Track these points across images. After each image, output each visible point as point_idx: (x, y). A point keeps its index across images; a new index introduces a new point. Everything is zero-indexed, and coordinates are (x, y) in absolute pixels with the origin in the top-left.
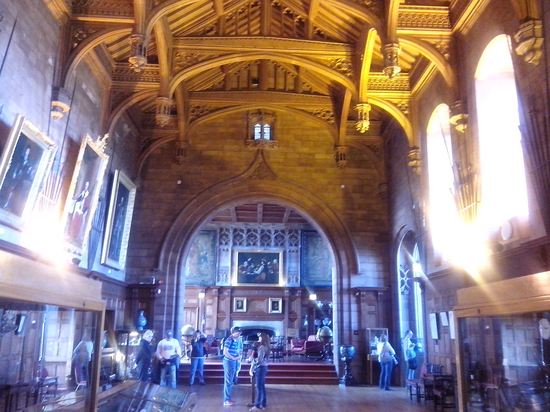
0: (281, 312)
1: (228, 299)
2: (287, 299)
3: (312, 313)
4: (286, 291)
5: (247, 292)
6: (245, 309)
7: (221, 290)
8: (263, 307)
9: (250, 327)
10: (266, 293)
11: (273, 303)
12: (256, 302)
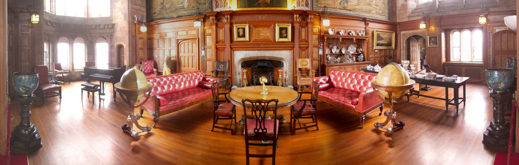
0: (290, 40)
1: (227, 26)
2: (297, 26)
3: (323, 41)
4: (295, 16)
5: (248, 18)
6: (247, 38)
7: (218, 16)
8: (268, 34)
9: (253, 58)
10: (272, 18)
11: (281, 29)
12: (261, 29)
